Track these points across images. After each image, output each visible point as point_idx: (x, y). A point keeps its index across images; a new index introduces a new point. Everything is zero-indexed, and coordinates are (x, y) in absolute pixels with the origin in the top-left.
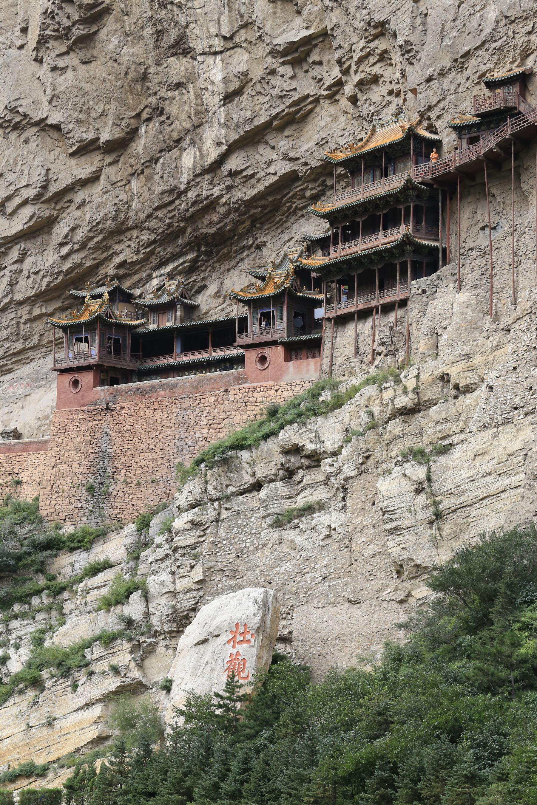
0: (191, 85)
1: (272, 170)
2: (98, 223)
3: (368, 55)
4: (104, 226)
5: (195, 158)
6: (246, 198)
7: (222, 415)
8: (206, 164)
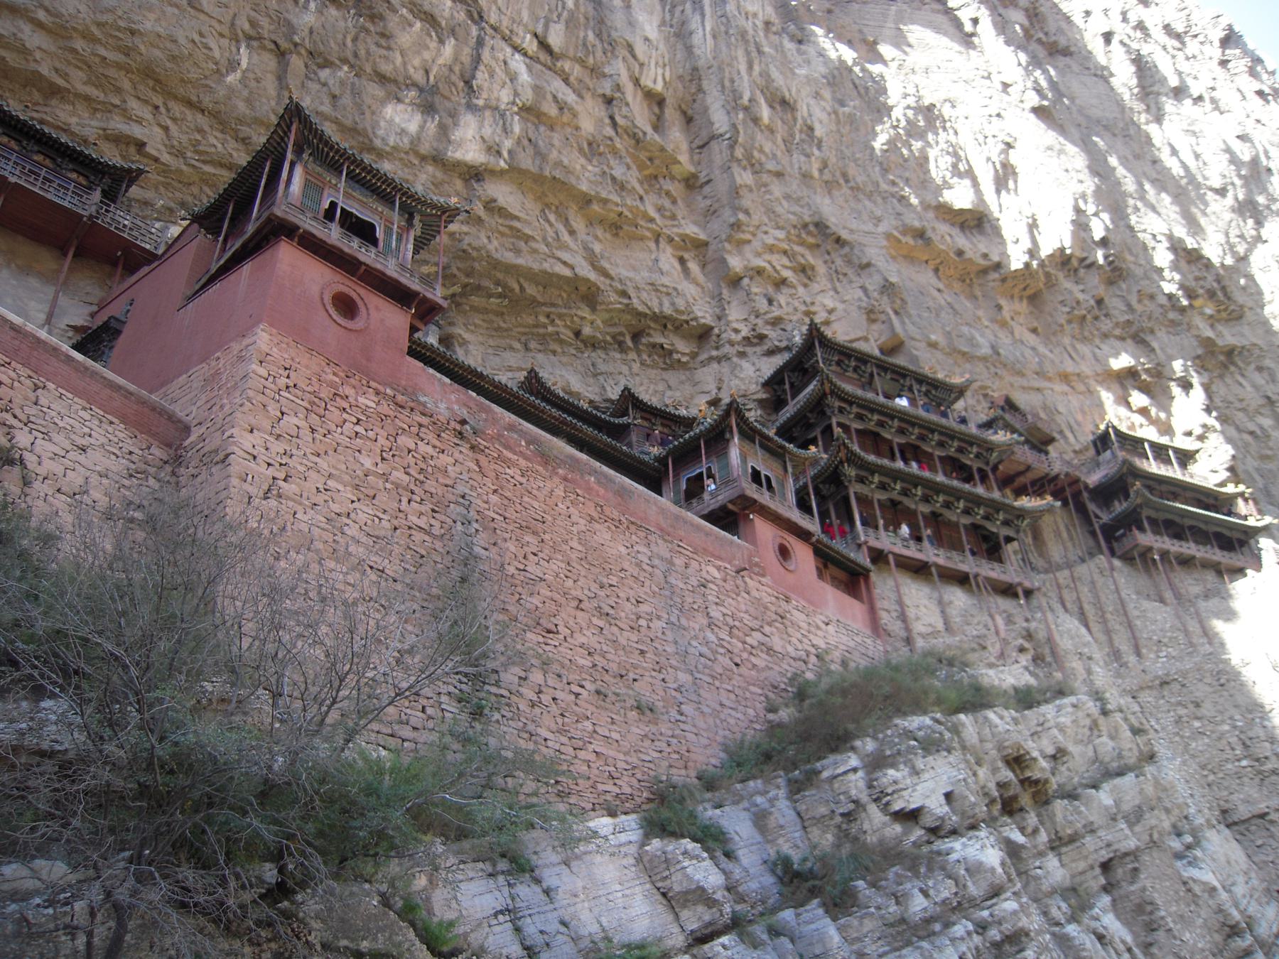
0: (453, 41)
2: (133, 32)
3: (785, 252)
4: (143, 48)
5: (422, 127)
6: (497, 256)
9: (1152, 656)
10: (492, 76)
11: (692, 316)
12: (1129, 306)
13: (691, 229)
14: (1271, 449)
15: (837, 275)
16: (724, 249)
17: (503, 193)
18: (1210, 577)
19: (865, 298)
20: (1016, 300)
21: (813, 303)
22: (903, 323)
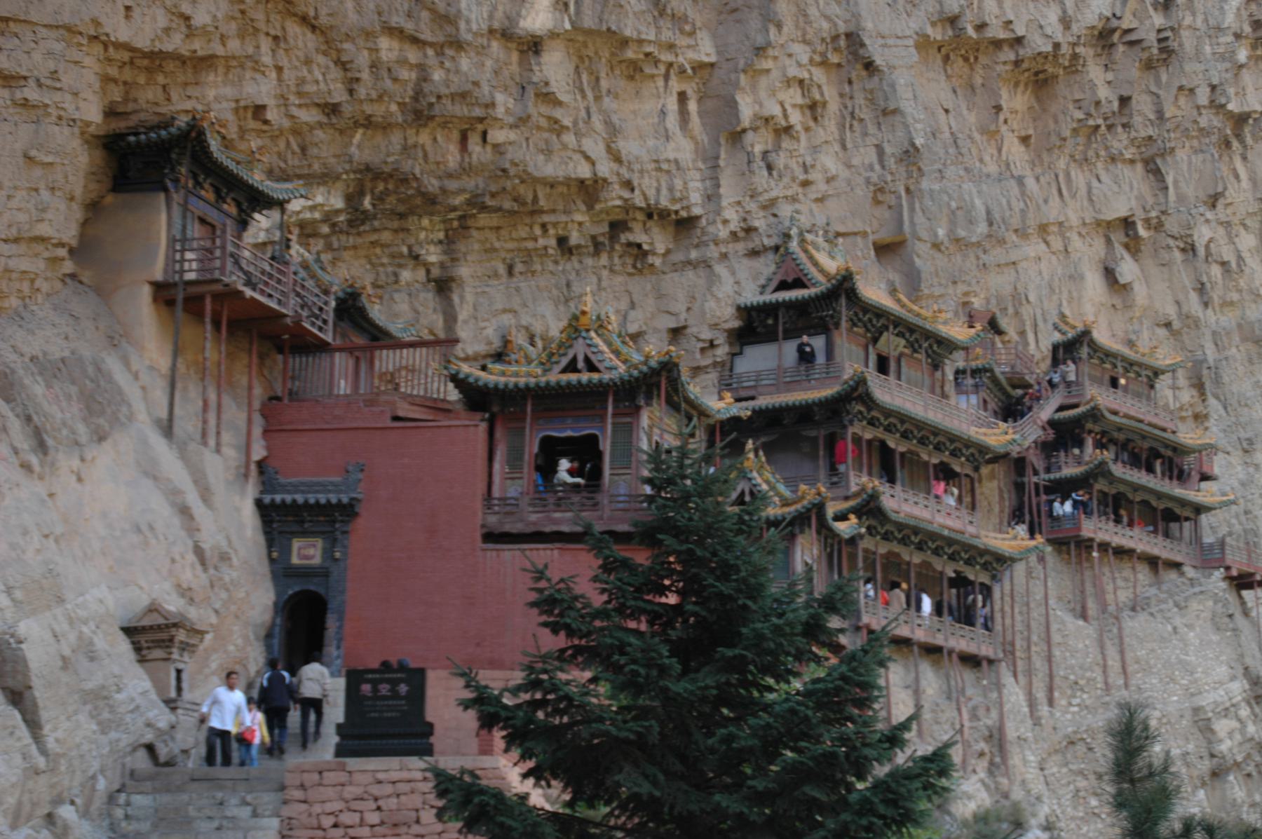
9: (1064, 702)
11: (685, 203)
12: (1160, 114)
13: (706, 51)
14: (1240, 291)
15: (849, 118)
16: (736, 85)
18: (1143, 574)
19: (877, 167)
20: (1021, 88)
22: (912, 210)
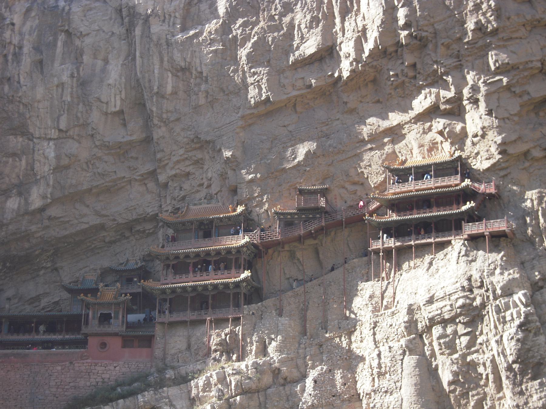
0: (25, 157)
1: (85, 220)
5: (19, 204)
7: (68, 380)
8: (30, 209)
10: (40, 163)
17: (53, 212)
21: (202, 179)
